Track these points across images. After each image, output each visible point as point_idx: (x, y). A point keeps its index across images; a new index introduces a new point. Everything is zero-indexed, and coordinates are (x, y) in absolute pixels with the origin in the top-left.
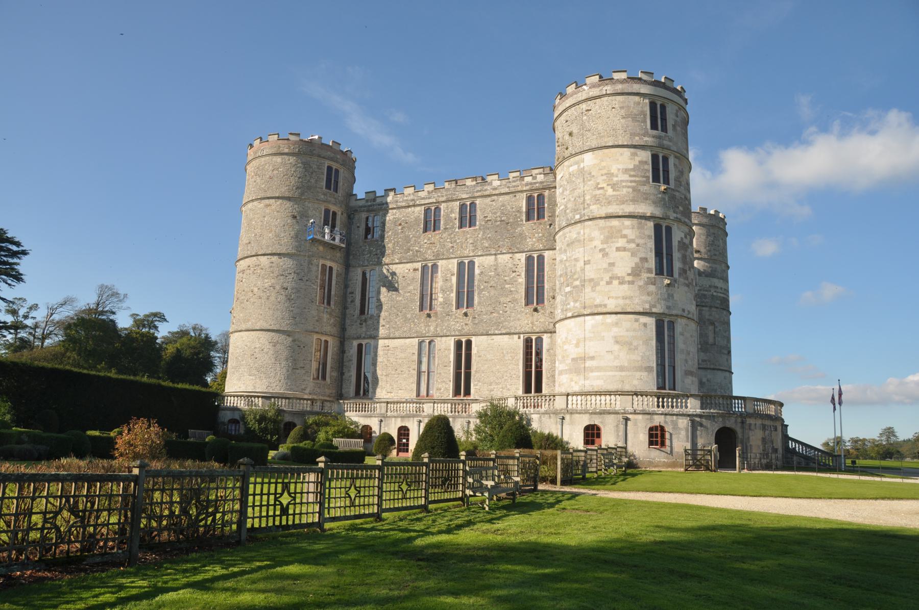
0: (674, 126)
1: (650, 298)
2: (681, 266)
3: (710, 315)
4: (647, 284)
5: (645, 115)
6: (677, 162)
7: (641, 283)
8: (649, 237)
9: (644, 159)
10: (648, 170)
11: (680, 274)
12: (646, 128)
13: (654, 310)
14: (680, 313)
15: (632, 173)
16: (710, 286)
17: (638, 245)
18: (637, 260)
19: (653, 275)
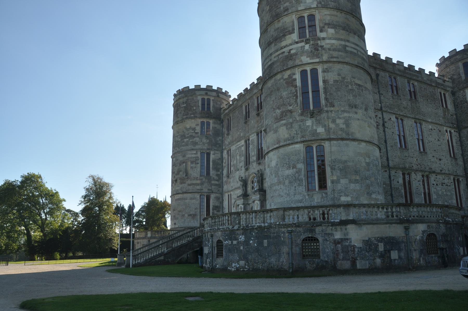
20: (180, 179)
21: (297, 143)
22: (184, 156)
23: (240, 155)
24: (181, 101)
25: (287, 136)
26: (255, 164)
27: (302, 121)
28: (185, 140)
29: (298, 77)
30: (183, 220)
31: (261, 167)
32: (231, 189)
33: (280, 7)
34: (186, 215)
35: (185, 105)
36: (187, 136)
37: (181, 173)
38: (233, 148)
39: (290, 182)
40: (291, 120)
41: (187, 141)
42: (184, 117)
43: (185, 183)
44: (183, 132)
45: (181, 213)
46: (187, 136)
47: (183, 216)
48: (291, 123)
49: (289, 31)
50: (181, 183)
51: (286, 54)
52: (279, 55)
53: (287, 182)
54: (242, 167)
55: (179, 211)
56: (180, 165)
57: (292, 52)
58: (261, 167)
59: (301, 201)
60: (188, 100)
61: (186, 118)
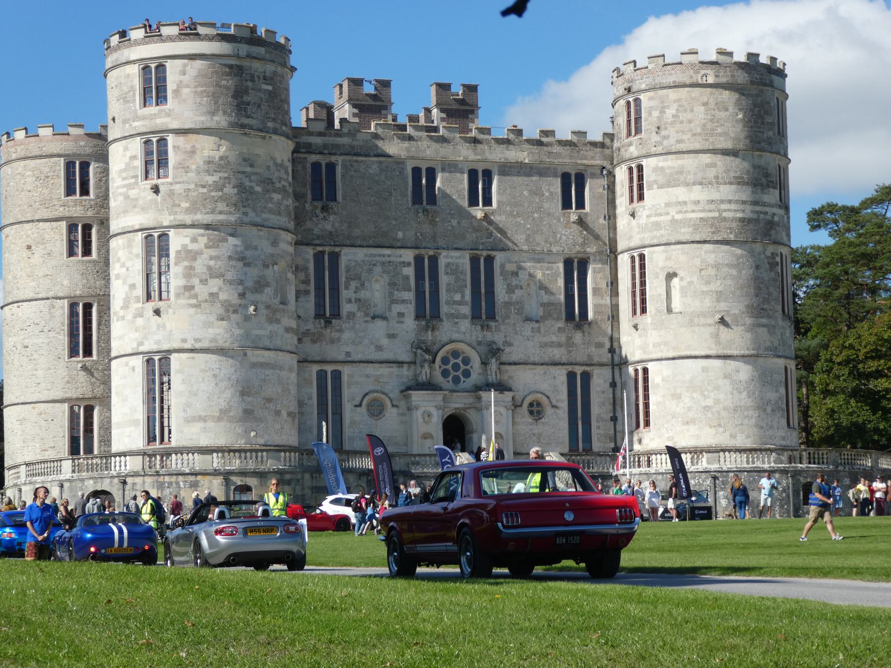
0: (176, 92)
1: (137, 335)
2: (182, 282)
3: (668, 258)
4: (135, 317)
5: (134, 91)
6: (181, 140)
7: (129, 317)
8: (137, 256)
9: (134, 153)
10: (136, 168)
11: (178, 296)
12: (136, 110)
13: (142, 349)
14: (176, 345)
15: (124, 175)
16: (668, 205)
17: (127, 269)
18: (127, 288)
19: (140, 305)
20: (268, 307)
21: (780, 357)
22: (275, 243)
23: (392, 284)
24: (257, 65)
25: (768, 344)
26: (465, 325)
27: (784, 328)
28: (277, 197)
29: (778, 259)
30: (278, 426)
31: (489, 336)
32: (342, 357)
33: (763, 132)
34: (284, 413)
35: (270, 88)
36: (278, 185)
37: (268, 290)
38: (349, 256)
39: (773, 411)
40: (773, 323)
41: (279, 203)
42: (270, 124)
43: (278, 321)
44: (268, 168)
45: (271, 406)
46: (278, 185)
47: (278, 413)
48: (774, 327)
49: (772, 182)
50: (271, 321)
51: (768, 217)
52: (761, 212)
53: (769, 409)
54: (401, 315)
55: (269, 400)
56: (266, 266)
57: (776, 219)
58: (489, 336)
59: (784, 438)
60: (275, 73)
61: (275, 132)
